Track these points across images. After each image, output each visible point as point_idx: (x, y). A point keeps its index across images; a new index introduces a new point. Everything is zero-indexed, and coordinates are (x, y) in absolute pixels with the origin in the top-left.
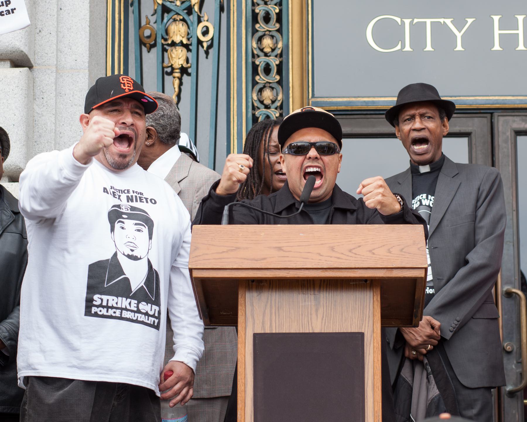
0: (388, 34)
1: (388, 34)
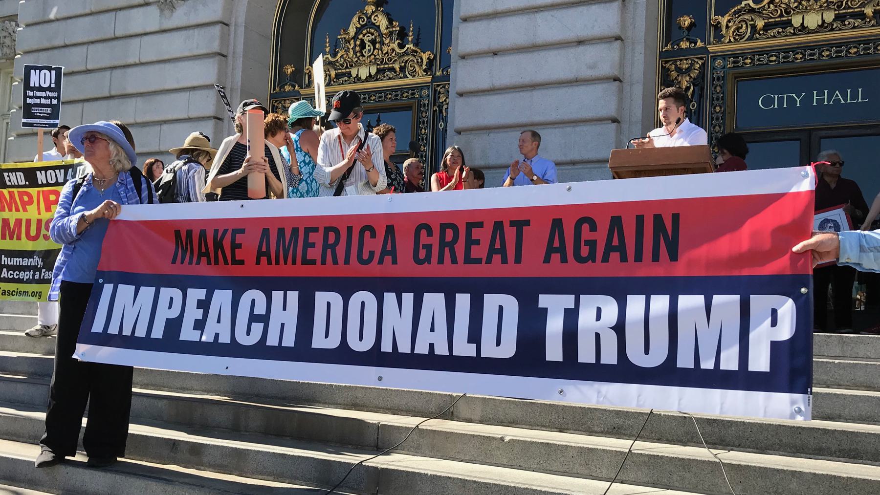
0: (768, 102)
1: (768, 102)
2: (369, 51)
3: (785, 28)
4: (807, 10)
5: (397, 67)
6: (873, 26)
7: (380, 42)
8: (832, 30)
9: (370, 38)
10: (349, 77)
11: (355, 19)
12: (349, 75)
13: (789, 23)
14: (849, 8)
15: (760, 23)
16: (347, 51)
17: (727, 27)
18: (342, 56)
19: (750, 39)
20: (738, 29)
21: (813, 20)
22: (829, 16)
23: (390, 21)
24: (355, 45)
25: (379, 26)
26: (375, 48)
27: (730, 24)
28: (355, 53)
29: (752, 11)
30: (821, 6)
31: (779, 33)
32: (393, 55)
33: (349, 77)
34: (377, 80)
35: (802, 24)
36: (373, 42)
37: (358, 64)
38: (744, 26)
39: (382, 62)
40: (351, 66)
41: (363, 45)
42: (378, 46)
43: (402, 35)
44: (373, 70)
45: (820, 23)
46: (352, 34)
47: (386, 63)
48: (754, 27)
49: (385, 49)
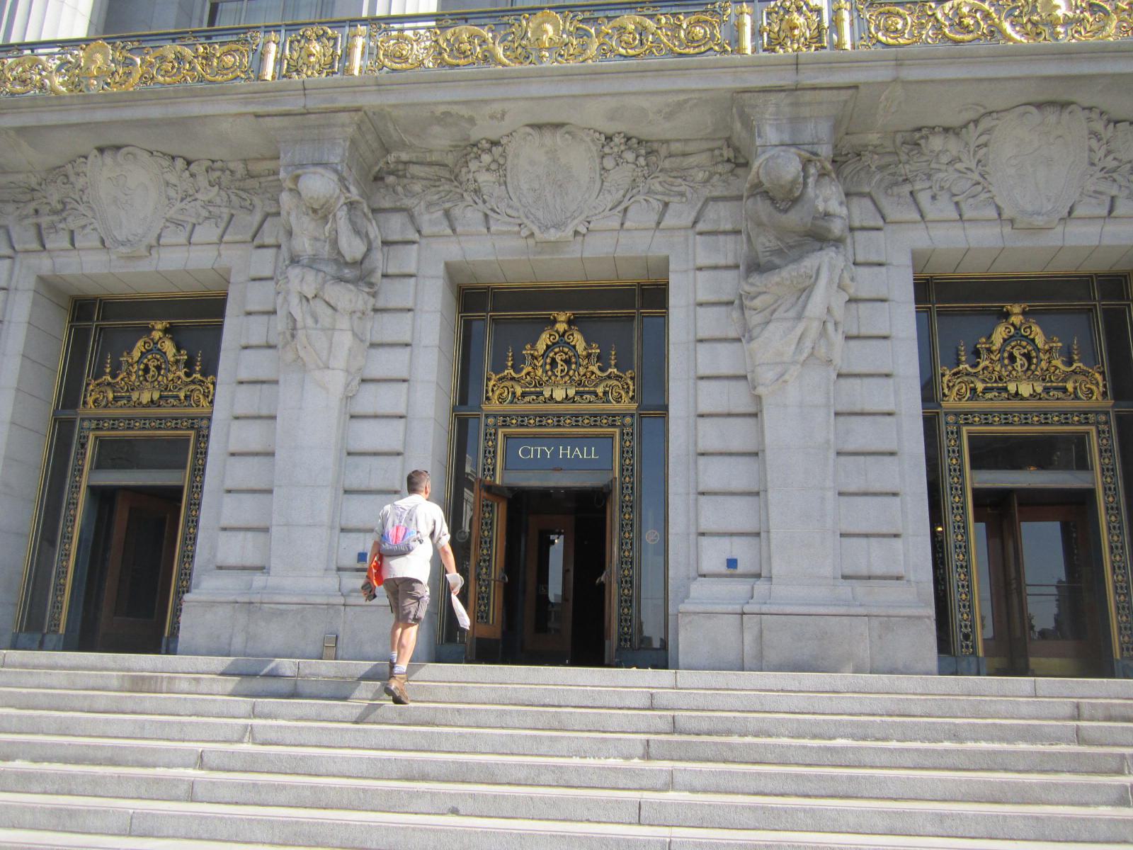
2: (153, 376)
3: (538, 397)
4: (556, 385)
5: (182, 395)
6: (603, 402)
7: (165, 369)
8: (574, 402)
9: (156, 363)
10: (129, 401)
11: (140, 344)
12: (129, 399)
13: (541, 393)
14: (586, 386)
15: (519, 391)
16: (129, 374)
17: (493, 390)
18: (122, 379)
19: (511, 402)
20: (501, 394)
21: (559, 394)
22: (571, 392)
23: (178, 349)
24: (139, 369)
25: (165, 353)
26: (159, 374)
27: (495, 389)
28: (138, 377)
29: (513, 379)
30: (565, 382)
31: (533, 400)
32: (179, 382)
33: (129, 401)
34: (159, 406)
35: (551, 395)
36: (158, 368)
37: (140, 389)
38: (506, 391)
39: (166, 389)
40: (133, 390)
41: (146, 370)
42: (162, 372)
43: (189, 364)
44: (156, 396)
45: (564, 396)
46: (136, 359)
47: (170, 391)
48: (514, 393)
49: (171, 376)
